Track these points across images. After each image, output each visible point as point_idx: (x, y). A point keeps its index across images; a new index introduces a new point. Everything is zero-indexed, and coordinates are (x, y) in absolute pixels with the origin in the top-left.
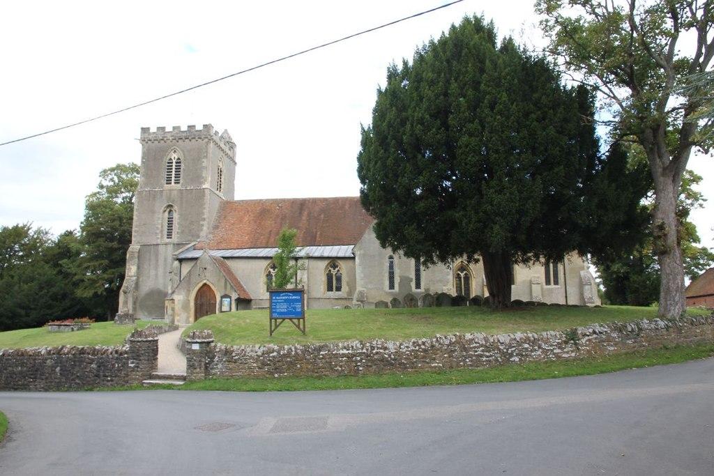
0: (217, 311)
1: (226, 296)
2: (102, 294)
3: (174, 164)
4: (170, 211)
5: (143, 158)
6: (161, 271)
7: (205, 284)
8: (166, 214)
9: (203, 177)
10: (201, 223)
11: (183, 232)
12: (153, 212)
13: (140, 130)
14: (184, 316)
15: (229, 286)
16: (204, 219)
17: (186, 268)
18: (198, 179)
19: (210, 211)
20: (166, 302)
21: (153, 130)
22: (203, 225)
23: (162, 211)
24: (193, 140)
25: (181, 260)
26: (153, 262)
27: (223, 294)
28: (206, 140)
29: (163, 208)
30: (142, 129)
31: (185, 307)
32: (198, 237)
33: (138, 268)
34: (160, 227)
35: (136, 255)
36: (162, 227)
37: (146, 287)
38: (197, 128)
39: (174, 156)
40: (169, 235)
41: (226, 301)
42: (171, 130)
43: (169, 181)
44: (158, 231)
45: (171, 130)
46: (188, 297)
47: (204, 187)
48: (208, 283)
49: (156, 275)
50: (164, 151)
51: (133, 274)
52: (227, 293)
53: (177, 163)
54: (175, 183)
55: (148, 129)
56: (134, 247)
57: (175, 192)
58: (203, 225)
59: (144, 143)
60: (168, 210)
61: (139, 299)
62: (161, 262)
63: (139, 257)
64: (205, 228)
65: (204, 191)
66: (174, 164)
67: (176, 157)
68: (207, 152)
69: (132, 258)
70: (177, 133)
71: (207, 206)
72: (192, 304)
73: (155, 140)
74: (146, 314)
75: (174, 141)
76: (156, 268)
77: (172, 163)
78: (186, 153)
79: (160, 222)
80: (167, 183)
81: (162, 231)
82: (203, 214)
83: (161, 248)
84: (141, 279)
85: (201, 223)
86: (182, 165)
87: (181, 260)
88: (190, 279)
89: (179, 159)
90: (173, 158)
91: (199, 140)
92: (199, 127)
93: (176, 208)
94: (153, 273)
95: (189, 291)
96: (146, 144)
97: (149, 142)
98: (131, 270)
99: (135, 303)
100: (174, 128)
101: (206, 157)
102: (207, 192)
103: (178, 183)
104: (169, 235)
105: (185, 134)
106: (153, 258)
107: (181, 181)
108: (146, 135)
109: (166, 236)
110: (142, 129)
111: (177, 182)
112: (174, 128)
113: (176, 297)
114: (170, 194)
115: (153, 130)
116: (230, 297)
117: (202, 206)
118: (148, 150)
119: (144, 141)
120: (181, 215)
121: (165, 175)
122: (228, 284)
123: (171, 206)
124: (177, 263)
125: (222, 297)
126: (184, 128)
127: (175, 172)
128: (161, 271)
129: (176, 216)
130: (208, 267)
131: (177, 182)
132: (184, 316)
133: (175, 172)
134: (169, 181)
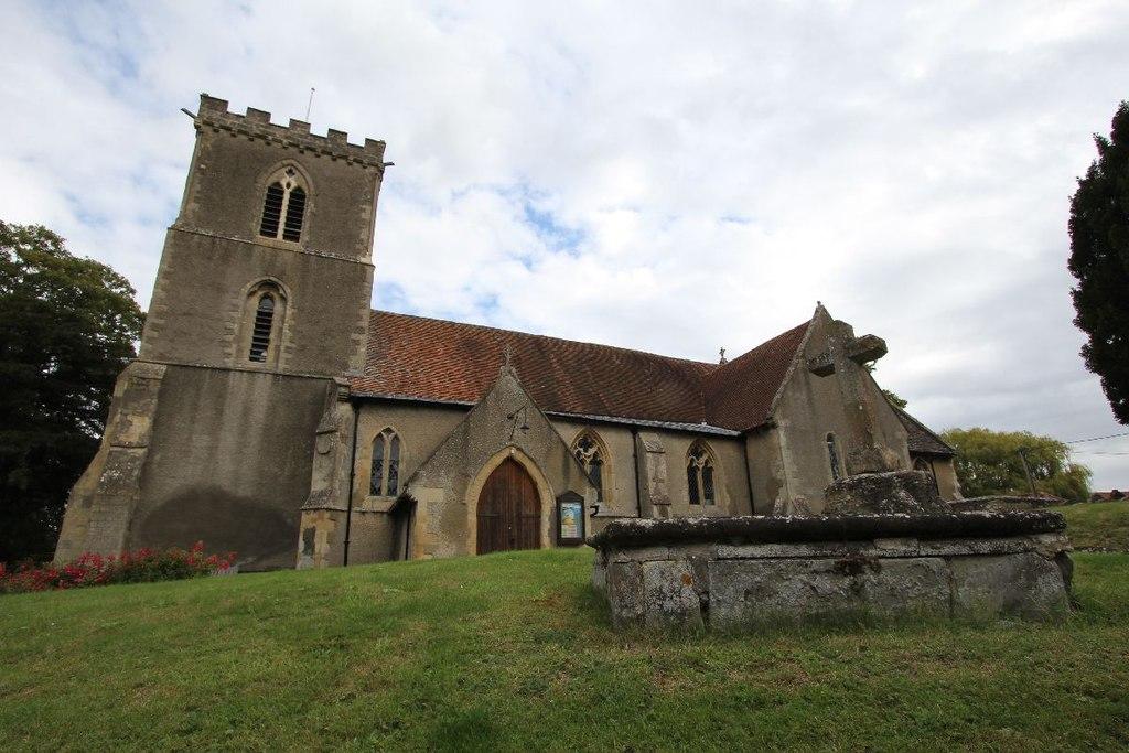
0: (546, 539)
7: (510, 460)
8: (255, 301)
9: (362, 242)
10: (354, 336)
11: (303, 348)
12: (220, 290)
22: (357, 342)
23: (245, 291)
24: (342, 162)
27: (560, 491)
29: (249, 286)
31: (451, 524)
32: (345, 366)
33: (156, 424)
34: (236, 327)
35: (155, 387)
36: (240, 330)
38: (350, 140)
39: (289, 182)
41: (571, 511)
43: (269, 228)
44: (230, 338)
48: (519, 457)
49: (213, 450)
50: (265, 162)
51: (134, 440)
54: (285, 237)
57: (288, 257)
58: (357, 342)
60: (261, 293)
63: (161, 395)
67: (294, 184)
72: (472, 519)
73: (240, 132)
76: (215, 428)
77: (282, 192)
81: (239, 339)
83: (234, 380)
84: (157, 457)
85: (354, 336)
86: (310, 207)
89: (299, 189)
90: (284, 183)
91: (355, 164)
94: (201, 441)
95: (464, 478)
96: (211, 133)
107: (304, 237)
108: (216, 115)
109: (247, 353)
110: (205, 97)
111: (292, 235)
116: (581, 501)
121: (259, 212)
125: (559, 500)
128: (228, 439)
131: (292, 235)
134: (269, 228)
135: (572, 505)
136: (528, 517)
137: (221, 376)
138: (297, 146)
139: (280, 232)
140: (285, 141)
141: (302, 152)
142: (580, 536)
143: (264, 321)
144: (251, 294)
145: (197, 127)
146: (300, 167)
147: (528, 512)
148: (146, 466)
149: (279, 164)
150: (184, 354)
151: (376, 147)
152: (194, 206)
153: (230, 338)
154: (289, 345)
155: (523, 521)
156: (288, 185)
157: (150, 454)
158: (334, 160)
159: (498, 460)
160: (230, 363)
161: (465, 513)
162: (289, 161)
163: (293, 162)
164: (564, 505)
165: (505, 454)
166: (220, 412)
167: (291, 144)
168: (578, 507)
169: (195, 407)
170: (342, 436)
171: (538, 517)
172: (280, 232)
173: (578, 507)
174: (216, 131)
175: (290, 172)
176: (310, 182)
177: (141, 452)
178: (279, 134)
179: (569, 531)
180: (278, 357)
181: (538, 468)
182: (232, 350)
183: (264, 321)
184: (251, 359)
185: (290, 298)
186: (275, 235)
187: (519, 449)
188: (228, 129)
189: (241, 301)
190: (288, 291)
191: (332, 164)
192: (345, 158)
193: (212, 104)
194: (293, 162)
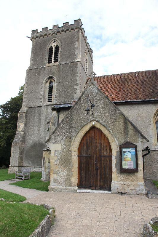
1: (128, 145)
2: (4, 146)
3: (54, 49)
4: (51, 82)
5: (32, 49)
6: (42, 127)
7: (93, 128)
8: (48, 84)
9: (75, 55)
10: (75, 87)
11: (60, 95)
12: (38, 83)
13: (31, 32)
14: (63, 173)
15: (131, 129)
16: (77, 85)
17: (62, 116)
18: (72, 55)
19: (81, 78)
20: (44, 153)
21: (40, 30)
22: (76, 89)
23: (44, 82)
24: (68, 32)
25: (58, 110)
26: (37, 120)
27: (123, 141)
28: (77, 30)
29: (45, 80)
30: (32, 31)
31: (65, 161)
32: (73, 98)
33: (26, 125)
34: (43, 93)
35: (24, 115)
36: (44, 94)
37: (32, 139)
39: (54, 45)
40: (50, 100)
41: (129, 154)
42: (52, 28)
43: (50, 61)
45: (52, 28)
46: (69, 146)
47: (76, 61)
48: (98, 125)
49: (39, 130)
50: (46, 42)
51: (21, 130)
52: (129, 139)
53: (55, 48)
54: (54, 62)
55: (37, 30)
56: (24, 110)
58: (76, 89)
59: (34, 39)
60: (49, 81)
61: (26, 150)
62: (43, 121)
63: (26, 117)
64: (78, 91)
65: (77, 64)
66: (54, 49)
68: (78, 37)
69: (22, 117)
70: (56, 29)
71: (79, 74)
72: (75, 158)
73: (41, 36)
74: (30, 163)
75: (54, 34)
77: (52, 49)
78: (63, 41)
79: (43, 89)
80: (49, 63)
81: (44, 97)
82: (77, 80)
83: (43, 109)
85: (75, 87)
86: (60, 50)
87: (58, 110)
88: (71, 121)
89: (57, 46)
90: (53, 46)
91: (72, 31)
92: (71, 22)
93: (55, 78)
94: (36, 129)
95: (70, 138)
97: (37, 38)
98: (21, 126)
99: (21, 153)
100: (54, 26)
101: (78, 40)
102: (79, 64)
103: (57, 61)
104: (50, 100)
105: (61, 29)
106: (37, 120)
107: (59, 60)
108: (35, 34)
109: (47, 100)
110: (32, 31)
111: (56, 61)
112: (54, 26)
113: (52, 146)
114: (51, 69)
115: (40, 30)
116: (136, 147)
117: (75, 74)
118: (36, 43)
119: (33, 38)
120: (59, 83)
121: (47, 57)
122: (130, 126)
123: (51, 78)
124: (55, 113)
125: (121, 147)
126: (61, 25)
127: (54, 55)
129: (55, 85)
130: (97, 103)
131: (56, 61)
132: (63, 173)
133: (54, 55)
134: (50, 61)
135: (129, 150)
136: (105, 156)
137: (39, 109)
138: (55, 33)
139: (53, 60)
140: (52, 33)
141: (56, 34)
142: (135, 167)
143: (51, 89)
144: (46, 82)
145: (31, 40)
146: (56, 39)
147: (105, 154)
148: (24, 137)
149: (51, 41)
150: (32, 104)
151: (78, 21)
152: (32, 62)
153: (41, 97)
154: (56, 95)
155: (103, 159)
156: (54, 46)
157: (25, 133)
158: (65, 32)
159: (87, 128)
160: (42, 104)
161: (71, 156)
162: (53, 39)
163: (54, 38)
164: (124, 150)
165: (90, 125)
166: (40, 120)
167: (53, 33)
168: (133, 150)
169: (34, 119)
170: (52, 123)
171: (111, 157)
172: (53, 60)
173: (134, 150)
174: (35, 39)
175: (55, 42)
176: (60, 42)
177: (22, 133)
178: (50, 32)
179: (128, 164)
180: (54, 101)
181: (108, 130)
182: (42, 100)
183: (51, 89)
184: (48, 102)
185: (56, 80)
186: (51, 62)
187: (97, 122)
188: (38, 37)
189: (43, 85)
190: (55, 78)
191: (65, 34)
192: (68, 30)
193: (34, 32)
194: (54, 38)
